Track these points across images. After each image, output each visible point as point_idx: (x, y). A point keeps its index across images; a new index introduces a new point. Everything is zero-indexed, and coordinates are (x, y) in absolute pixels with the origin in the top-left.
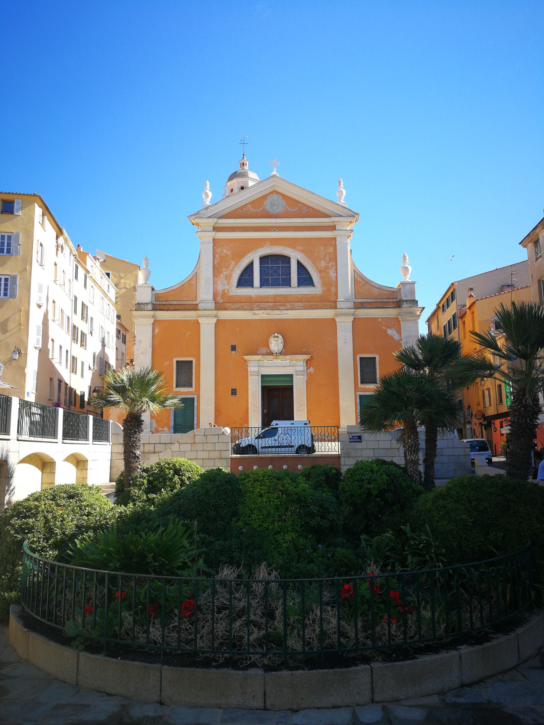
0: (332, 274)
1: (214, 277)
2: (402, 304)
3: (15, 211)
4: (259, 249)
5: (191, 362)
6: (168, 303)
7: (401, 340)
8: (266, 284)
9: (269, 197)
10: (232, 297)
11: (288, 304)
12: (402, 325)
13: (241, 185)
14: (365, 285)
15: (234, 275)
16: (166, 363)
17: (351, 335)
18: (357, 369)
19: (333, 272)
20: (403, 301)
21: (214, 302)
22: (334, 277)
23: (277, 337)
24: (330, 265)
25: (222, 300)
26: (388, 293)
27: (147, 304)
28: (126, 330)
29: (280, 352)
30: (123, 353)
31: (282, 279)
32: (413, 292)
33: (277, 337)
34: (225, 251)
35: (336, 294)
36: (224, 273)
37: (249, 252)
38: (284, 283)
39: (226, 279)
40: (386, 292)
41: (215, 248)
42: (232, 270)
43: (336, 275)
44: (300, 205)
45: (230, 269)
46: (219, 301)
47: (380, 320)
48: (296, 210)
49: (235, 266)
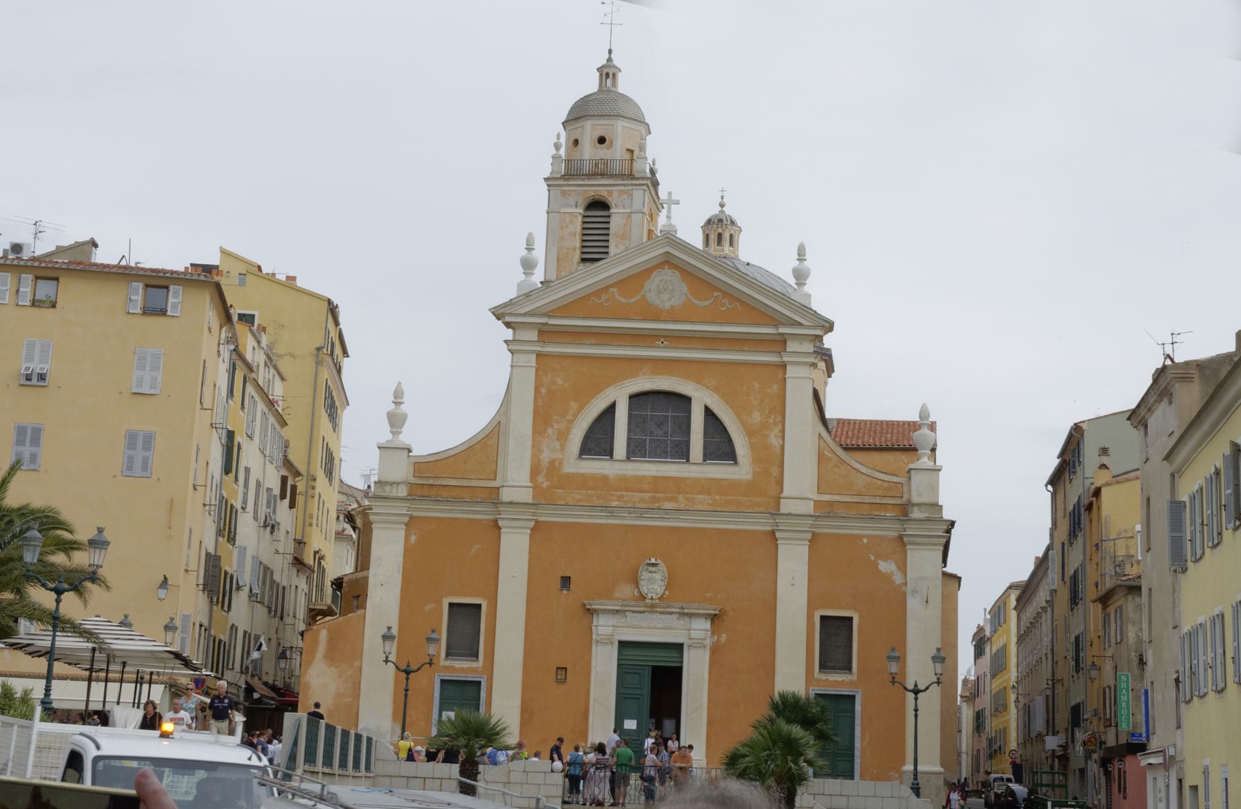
0: (774, 441)
1: (534, 433)
2: (910, 511)
3: (169, 309)
5: (479, 606)
6: (439, 483)
7: (906, 583)
10: (568, 475)
11: (681, 498)
12: (909, 553)
13: (600, 133)
14: (838, 467)
15: (574, 431)
16: (429, 607)
17: (805, 568)
19: (776, 436)
20: (914, 505)
21: (531, 485)
22: (778, 448)
24: (771, 421)
27: (398, 484)
28: (297, 474)
29: (660, 595)
30: (288, 532)
32: (935, 488)
34: (560, 382)
38: (677, 452)
39: (558, 439)
40: (879, 483)
42: (571, 422)
43: (781, 443)
44: (716, 294)
45: (568, 418)
46: (542, 483)
47: (865, 541)
48: (707, 303)
49: (579, 413)
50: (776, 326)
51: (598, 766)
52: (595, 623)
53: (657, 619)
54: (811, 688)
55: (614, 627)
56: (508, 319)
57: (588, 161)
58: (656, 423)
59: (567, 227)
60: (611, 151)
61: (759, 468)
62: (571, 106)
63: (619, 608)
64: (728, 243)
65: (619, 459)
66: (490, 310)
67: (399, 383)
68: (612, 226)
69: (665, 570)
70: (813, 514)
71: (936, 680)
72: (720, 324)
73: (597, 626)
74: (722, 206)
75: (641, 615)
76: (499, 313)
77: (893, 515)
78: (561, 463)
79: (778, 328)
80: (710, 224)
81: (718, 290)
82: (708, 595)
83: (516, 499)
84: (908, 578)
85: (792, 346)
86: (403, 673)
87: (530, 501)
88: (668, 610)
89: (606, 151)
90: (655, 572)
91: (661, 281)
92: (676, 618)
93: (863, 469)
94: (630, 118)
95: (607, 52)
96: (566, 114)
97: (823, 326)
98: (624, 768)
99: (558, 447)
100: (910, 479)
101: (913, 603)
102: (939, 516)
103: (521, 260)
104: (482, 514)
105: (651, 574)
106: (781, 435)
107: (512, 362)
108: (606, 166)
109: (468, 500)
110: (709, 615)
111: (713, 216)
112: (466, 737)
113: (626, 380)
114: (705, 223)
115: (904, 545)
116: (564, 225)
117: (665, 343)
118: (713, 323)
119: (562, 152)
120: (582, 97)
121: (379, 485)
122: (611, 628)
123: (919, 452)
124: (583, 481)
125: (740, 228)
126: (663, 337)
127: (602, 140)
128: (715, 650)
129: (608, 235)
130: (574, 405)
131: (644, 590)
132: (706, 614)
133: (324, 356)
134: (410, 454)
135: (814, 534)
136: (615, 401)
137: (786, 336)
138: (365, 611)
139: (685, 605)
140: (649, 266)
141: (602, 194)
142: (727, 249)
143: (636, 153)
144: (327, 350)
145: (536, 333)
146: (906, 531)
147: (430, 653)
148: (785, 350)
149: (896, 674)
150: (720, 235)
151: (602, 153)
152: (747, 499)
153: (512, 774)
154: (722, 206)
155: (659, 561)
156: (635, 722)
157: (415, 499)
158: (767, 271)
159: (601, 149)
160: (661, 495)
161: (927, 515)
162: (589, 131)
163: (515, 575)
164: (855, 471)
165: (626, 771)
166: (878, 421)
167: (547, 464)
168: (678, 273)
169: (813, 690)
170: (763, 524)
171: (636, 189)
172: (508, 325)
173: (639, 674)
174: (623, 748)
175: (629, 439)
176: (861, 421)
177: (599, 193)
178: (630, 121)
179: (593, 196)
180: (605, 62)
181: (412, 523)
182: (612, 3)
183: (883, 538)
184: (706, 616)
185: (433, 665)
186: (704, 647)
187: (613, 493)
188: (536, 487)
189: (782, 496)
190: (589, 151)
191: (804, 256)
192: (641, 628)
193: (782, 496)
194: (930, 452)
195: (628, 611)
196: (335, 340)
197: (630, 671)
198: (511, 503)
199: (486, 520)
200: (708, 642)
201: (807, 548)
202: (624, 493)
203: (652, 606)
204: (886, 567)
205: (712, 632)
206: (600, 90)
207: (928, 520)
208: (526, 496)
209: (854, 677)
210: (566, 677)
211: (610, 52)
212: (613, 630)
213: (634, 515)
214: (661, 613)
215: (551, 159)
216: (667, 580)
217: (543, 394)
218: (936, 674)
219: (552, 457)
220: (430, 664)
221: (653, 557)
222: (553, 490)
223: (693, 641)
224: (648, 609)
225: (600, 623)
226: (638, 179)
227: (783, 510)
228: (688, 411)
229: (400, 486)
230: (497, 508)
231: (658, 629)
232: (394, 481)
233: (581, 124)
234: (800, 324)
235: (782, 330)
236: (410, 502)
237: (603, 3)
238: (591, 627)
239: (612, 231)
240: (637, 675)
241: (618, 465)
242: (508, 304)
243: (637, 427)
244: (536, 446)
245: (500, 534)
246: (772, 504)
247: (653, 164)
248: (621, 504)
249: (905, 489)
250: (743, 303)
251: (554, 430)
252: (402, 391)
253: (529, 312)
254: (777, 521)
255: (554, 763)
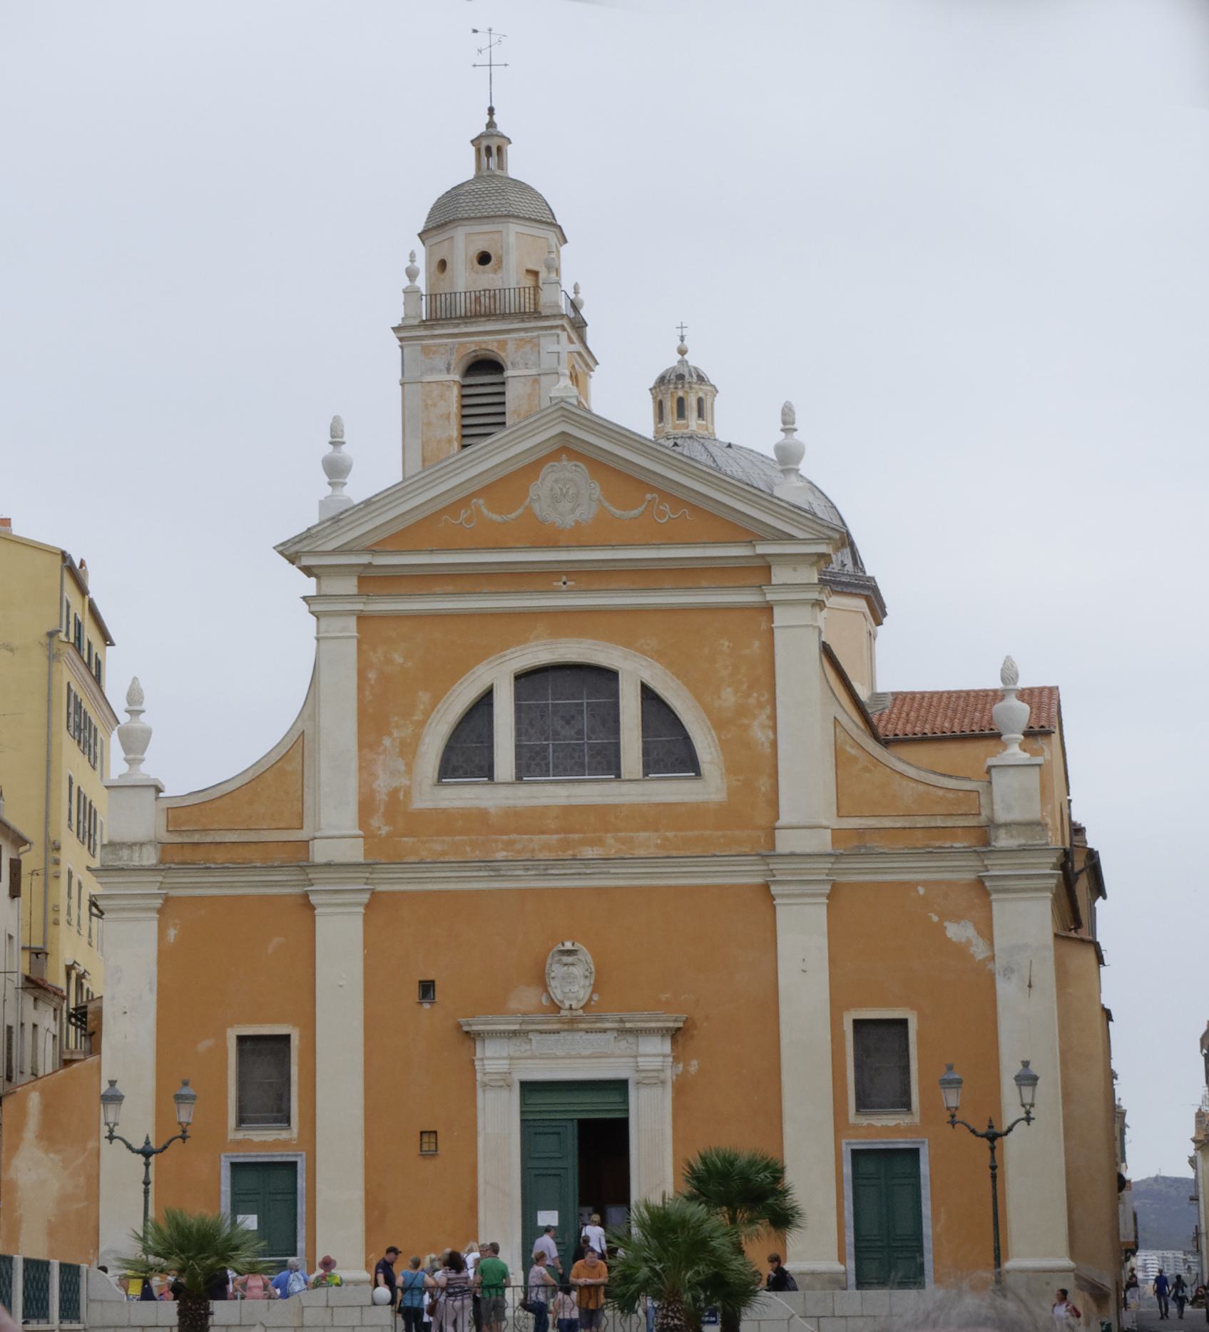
0: (759, 734)
1: (362, 745)
2: (993, 838)
4: (512, 650)
5: (286, 1039)
6: (209, 839)
7: (992, 958)
8: (538, 765)
9: (544, 471)
10: (421, 814)
11: (610, 839)
12: (995, 906)
15: (427, 740)
16: (205, 1044)
17: (824, 942)
18: (845, 1060)
20: (999, 826)
21: (361, 833)
22: (767, 745)
23: (570, 953)
24: (752, 701)
25: (385, 825)
26: (951, 795)
27: (142, 844)
29: (582, 1003)
31: (591, 747)
33: (570, 953)
34: (398, 659)
35: (774, 803)
36: (396, 733)
37: (479, 659)
38: (600, 763)
39: (401, 754)
40: (941, 793)
41: (365, 647)
42: (422, 724)
44: (649, 496)
45: (415, 718)
47: (921, 891)
48: (635, 512)
49: (433, 710)
50: (750, 543)
51: (451, 1290)
52: (479, 1055)
53: (582, 1042)
54: (844, 1141)
55: (511, 1058)
56: (306, 561)
57: (463, 294)
58: (563, 717)
59: (435, 405)
60: (500, 275)
61: (738, 780)
62: (431, 206)
63: (516, 1027)
64: (695, 414)
65: (502, 781)
66: (274, 548)
67: (135, 679)
68: (509, 398)
69: (589, 958)
70: (833, 852)
71: (1024, 1116)
72: (658, 546)
73: (482, 1059)
74: (682, 352)
75: (555, 1037)
76: (292, 552)
77: (966, 845)
78: (408, 793)
79: (754, 546)
80: (664, 384)
81: (653, 489)
82: (664, 997)
83: (339, 859)
84: (996, 948)
85: (780, 575)
86: (140, 1155)
87: (361, 860)
88: (599, 1025)
89: (491, 276)
90: (573, 964)
91: (556, 481)
92: (613, 1039)
93: (911, 772)
94: (530, 219)
95: (487, 112)
96: (425, 220)
97: (830, 538)
98: (493, 1291)
99: (403, 768)
100: (990, 783)
101: (1006, 990)
102: (1043, 842)
103: (323, 462)
104: (283, 885)
105: (566, 968)
106: (771, 723)
107: (318, 633)
108: (492, 300)
109: (259, 865)
110: (668, 1029)
111: (667, 370)
112: (183, 1256)
113: (508, 649)
114: (656, 383)
115: (986, 893)
116: (430, 402)
117: (568, 583)
118: (646, 545)
119: (421, 283)
120: (449, 189)
121: (108, 849)
122: (507, 1062)
123: (1003, 737)
124: (444, 822)
125: (714, 387)
126: (566, 573)
127: (484, 258)
128: (681, 1088)
129: (504, 413)
130: (424, 697)
131: (557, 994)
132: (662, 1029)
133: (61, 646)
134: (161, 795)
135: (835, 885)
136: (492, 685)
137: (768, 559)
138: (100, 1057)
139: (625, 1016)
140: (533, 458)
141: (489, 347)
142: (693, 422)
143: (542, 276)
144: (67, 635)
145: (355, 581)
146: (988, 871)
147: (182, 1120)
148: (769, 583)
149: (957, 1108)
150: (681, 402)
151: (487, 279)
152: (719, 833)
153: (307, 1311)
154: (682, 352)
155: (578, 946)
156: (556, 1213)
157: (170, 868)
158: (762, 456)
159: (484, 272)
160: (576, 836)
161: (1023, 842)
162: (463, 244)
163: (341, 983)
164: (897, 776)
165: (497, 1295)
166: (962, 691)
167: (386, 798)
168: (586, 470)
169: (847, 1144)
170: (747, 875)
171: (545, 336)
172: (308, 571)
173: (558, 1134)
174: (489, 1259)
175: (518, 747)
176: (933, 694)
177: (484, 346)
178: (528, 223)
179: (475, 351)
180: (484, 129)
181: (168, 908)
182: (490, 30)
183: (950, 884)
184: (663, 1032)
185: (187, 1140)
186: (663, 1082)
187: (494, 837)
188: (369, 836)
189: (778, 824)
190: (464, 278)
191: (794, 423)
192: (557, 1058)
193: (778, 824)
194: (1022, 737)
195: (532, 1031)
196: (83, 619)
197: (541, 1130)
198: (328, 865)
199: (290, 895)
200: (669, 1075)
201: (825, 907)
202: (513, 836)
203: (572, 1021)
204: (957, 931)
205: (674, 1057)
206: (478, 177)
207: (1022, 849)
208: (354, 851)
209: (915, 1118)
210: (436, 1147)
211: (491, 111)
212: (510, 1064)
213: (533, 872)
214: (587, 1032)
215: (403, 294)
216: (593, 975)
217: (373, 682)
218: (1023, 1105)
219: (394, 785)
220: (184, 1138)
221: (568, 939)
222: (397, 839)
223: (644, 1075)
224: (566, 1027)
225: (488, 1054)
226: (547, 317)
227: (781, 847)
228: (615, 694)
229: (144, 850)
230: (307, 874)
231: (583, 1058)
232: (133, 840)
233: (446, 235)
234: (791, 538)
235: (761, 549)
236: (163, 873)
237: (475, 31)
238: (473, 1061)
239: (509, 408)
240: (556, 1136)
241: (503, 792)
242: (304, 536)
243: (532, 725)
244: (365, 768)
245: (314, 917)
246: (762, 841)
247: (576, 292)
248: (510, 855)
249: (983, 800)
250: (694, 508)
251: (393, 740)
252: (140, 692)
253: (341, 546)
254: (771, 867)
255: (378, 1289)
